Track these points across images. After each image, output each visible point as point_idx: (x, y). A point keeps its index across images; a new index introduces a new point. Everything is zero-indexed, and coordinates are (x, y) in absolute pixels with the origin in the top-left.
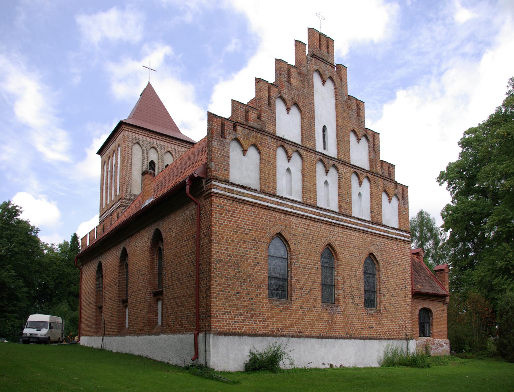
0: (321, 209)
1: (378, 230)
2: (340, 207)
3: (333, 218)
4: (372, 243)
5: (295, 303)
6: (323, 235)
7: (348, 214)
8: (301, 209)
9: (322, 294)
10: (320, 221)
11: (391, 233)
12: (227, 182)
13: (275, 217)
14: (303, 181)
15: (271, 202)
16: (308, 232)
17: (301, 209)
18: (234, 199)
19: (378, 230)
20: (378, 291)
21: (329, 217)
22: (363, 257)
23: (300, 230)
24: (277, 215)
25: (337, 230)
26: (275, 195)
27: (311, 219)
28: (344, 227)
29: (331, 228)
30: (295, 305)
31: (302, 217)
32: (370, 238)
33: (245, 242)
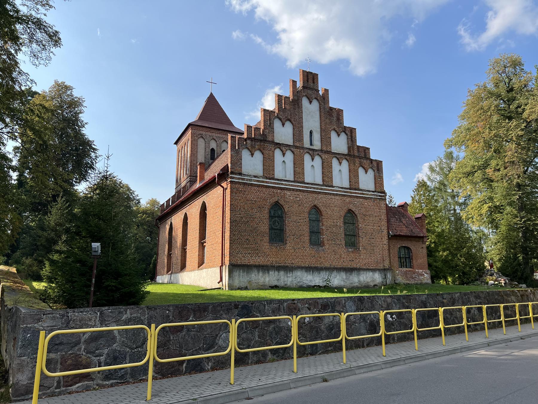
0: (308, 184)
1: (355, 193)
2: (323, 181)
3: (317, 189)
4: (350, 203)
5: (288, 244)
6: (309, 200)
7: (330, 184)
8: (292, 186)
9: (310, 239)
10: (307, 191)
11: (367, 194)
12: (240, 174)
13: (274, 192)
14: (294, 167)
15: (271, 183)
16: (298, 199)
17: (292, 186)
18: (245, 184)
19: (355, 193)
20: (357, 235)
21: (314, 188)
22: (343, 213)
23: (292, 198)
24: (275, 191)
25: (320, 196)
26: (273, 179)
27: (300, 190)
28: (326, 194)
29: (316, 196)
30: (288, 246)
31: (293, 190)
32: (348, 200)
33: (252, 209)
